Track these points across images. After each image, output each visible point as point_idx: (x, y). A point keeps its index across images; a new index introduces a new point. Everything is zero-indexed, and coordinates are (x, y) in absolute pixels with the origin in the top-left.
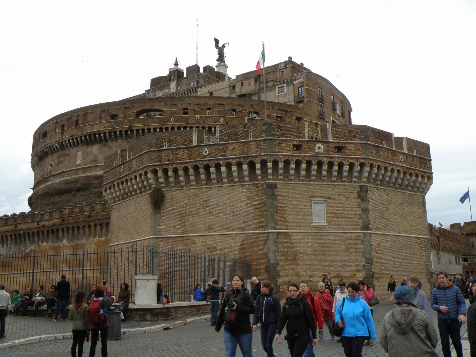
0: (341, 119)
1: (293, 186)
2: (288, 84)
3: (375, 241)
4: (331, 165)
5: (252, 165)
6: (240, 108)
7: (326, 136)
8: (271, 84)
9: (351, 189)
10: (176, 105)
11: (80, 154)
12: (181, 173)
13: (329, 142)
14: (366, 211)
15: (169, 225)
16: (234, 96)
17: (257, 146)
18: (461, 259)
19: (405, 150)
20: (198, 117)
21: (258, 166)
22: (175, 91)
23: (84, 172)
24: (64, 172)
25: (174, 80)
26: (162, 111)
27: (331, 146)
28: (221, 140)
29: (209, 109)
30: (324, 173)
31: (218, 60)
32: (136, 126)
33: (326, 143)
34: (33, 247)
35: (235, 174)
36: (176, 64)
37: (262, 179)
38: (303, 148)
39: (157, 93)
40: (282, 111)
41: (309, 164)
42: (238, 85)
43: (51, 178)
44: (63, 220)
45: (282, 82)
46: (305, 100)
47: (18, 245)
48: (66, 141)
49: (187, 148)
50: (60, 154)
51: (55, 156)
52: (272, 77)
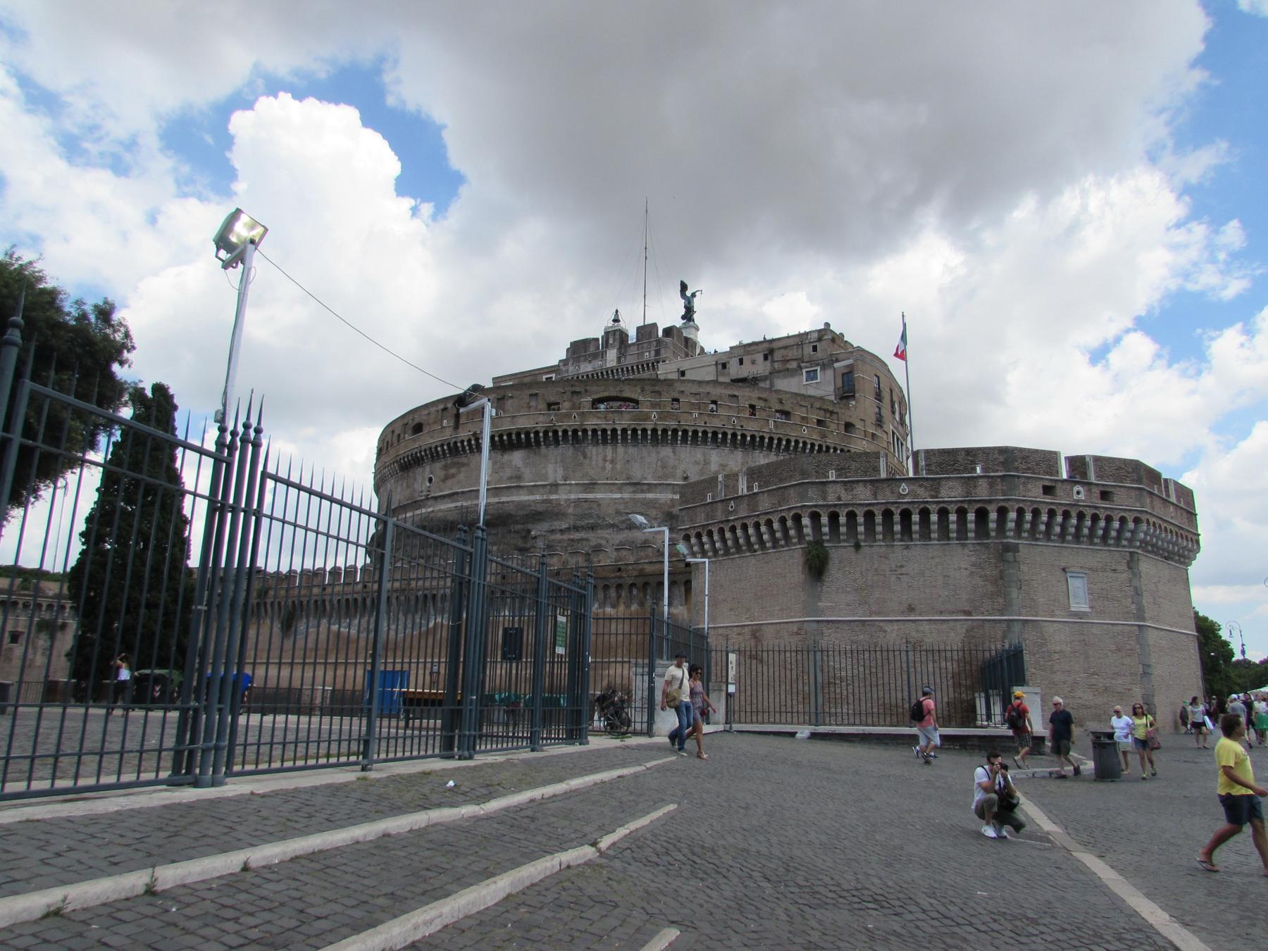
1: (1039, 549)
2: (824, 367)
5: (982, 515)
6: (762, 404)
10: (659, 393)
13: (1091, 484)
14: (1138, 593)
15: (839, 601)
16: (721, 379)
17: (991, 485)
19: (1173, 499)
20: (696, 414)
21: (993, 516)
22: (614, 364)
24: (457, 493)
25: (614, 347)
26: (637, 402)
28: (929, 471)
29: (714, 402)
31: (683, 318)
32: (591, 423)
35: (953, 527)
36: (616, 320)
37: (996, 538)
38: (1059, 492)
39: (582, 366)
41: (1066, 515)
42: (734, 363)
43: (430, 503)
44: (504, 577)
45: (812, 362)
48: (462, 442)
49: (871, 482)
50: (449, 461)
51: (438, 465)
52: (794, 353)
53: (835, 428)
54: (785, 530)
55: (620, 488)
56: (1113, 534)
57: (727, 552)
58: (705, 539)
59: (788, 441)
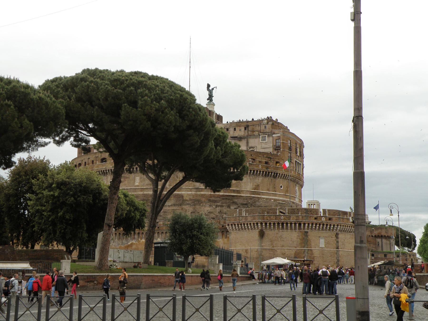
0: (300, 159)
2: (269, 136)
3: (340, 253)
4: (327, 225)
5: (300, 224)
7: (326, 214)
8: (256, 133)
9: (333, 234)
11: (138, 179)
12: (272, 225)
14: (338, 242)
18: (369, 254)
21: (302, 225)
23: (141, 191)
27: (328, 218)
28: (288, 214)
30: (325, 228)
31: (208, 100)
33: (326, 217)
34: (134, 242)
35: (293, 227)
40: (268, 158)
46: (281, 150)
47: (120, 240)
52: (258, 128)
53: (272, 164)
54: (254, 226)
55: (191, 191)
56: (332, 228)
57: (239, 230)
58: (233, 226)
59: (254, 171)
